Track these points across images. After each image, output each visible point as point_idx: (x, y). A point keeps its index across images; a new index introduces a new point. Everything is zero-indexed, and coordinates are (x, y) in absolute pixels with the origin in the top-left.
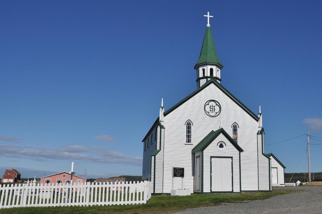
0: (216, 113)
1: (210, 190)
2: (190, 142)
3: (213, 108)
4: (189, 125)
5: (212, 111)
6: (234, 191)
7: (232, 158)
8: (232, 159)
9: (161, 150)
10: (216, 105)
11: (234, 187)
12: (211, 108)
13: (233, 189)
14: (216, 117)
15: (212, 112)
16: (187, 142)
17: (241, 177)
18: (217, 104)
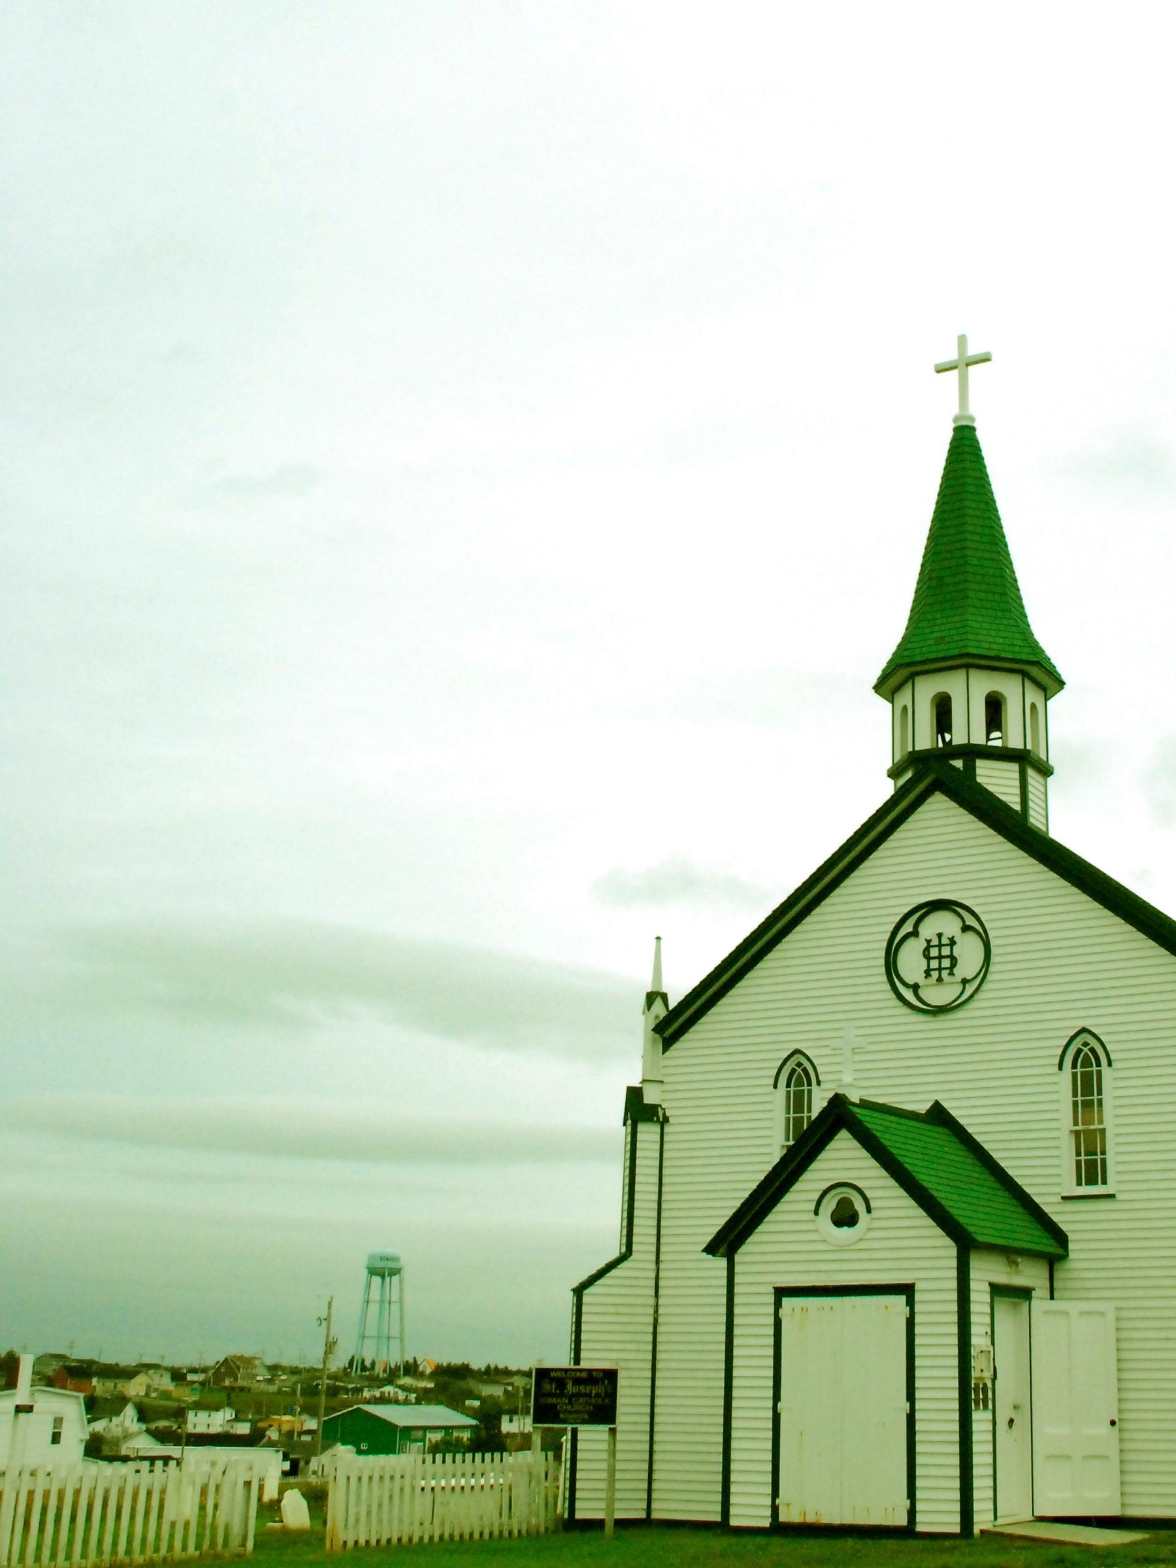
0: (965, 982)
1: (768, 1512)
2: (1104, 1182)
3: (946, 951)
4: (1086, 1063)
5: (935, 974)
6: (919, 1528)
7: (907, 1290)
8: (911, 1303)
9: (634, 1256)
10: (915, 933)
11: (919, 1494)
12: (928, 958)
13: (912, 1513)
14: (960, 1014)
15: (940, 980)
16: (1079, 1183)
17: (734, 1424)
18: (908, 928)
